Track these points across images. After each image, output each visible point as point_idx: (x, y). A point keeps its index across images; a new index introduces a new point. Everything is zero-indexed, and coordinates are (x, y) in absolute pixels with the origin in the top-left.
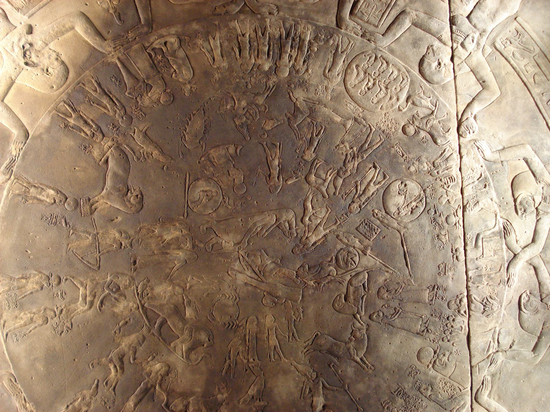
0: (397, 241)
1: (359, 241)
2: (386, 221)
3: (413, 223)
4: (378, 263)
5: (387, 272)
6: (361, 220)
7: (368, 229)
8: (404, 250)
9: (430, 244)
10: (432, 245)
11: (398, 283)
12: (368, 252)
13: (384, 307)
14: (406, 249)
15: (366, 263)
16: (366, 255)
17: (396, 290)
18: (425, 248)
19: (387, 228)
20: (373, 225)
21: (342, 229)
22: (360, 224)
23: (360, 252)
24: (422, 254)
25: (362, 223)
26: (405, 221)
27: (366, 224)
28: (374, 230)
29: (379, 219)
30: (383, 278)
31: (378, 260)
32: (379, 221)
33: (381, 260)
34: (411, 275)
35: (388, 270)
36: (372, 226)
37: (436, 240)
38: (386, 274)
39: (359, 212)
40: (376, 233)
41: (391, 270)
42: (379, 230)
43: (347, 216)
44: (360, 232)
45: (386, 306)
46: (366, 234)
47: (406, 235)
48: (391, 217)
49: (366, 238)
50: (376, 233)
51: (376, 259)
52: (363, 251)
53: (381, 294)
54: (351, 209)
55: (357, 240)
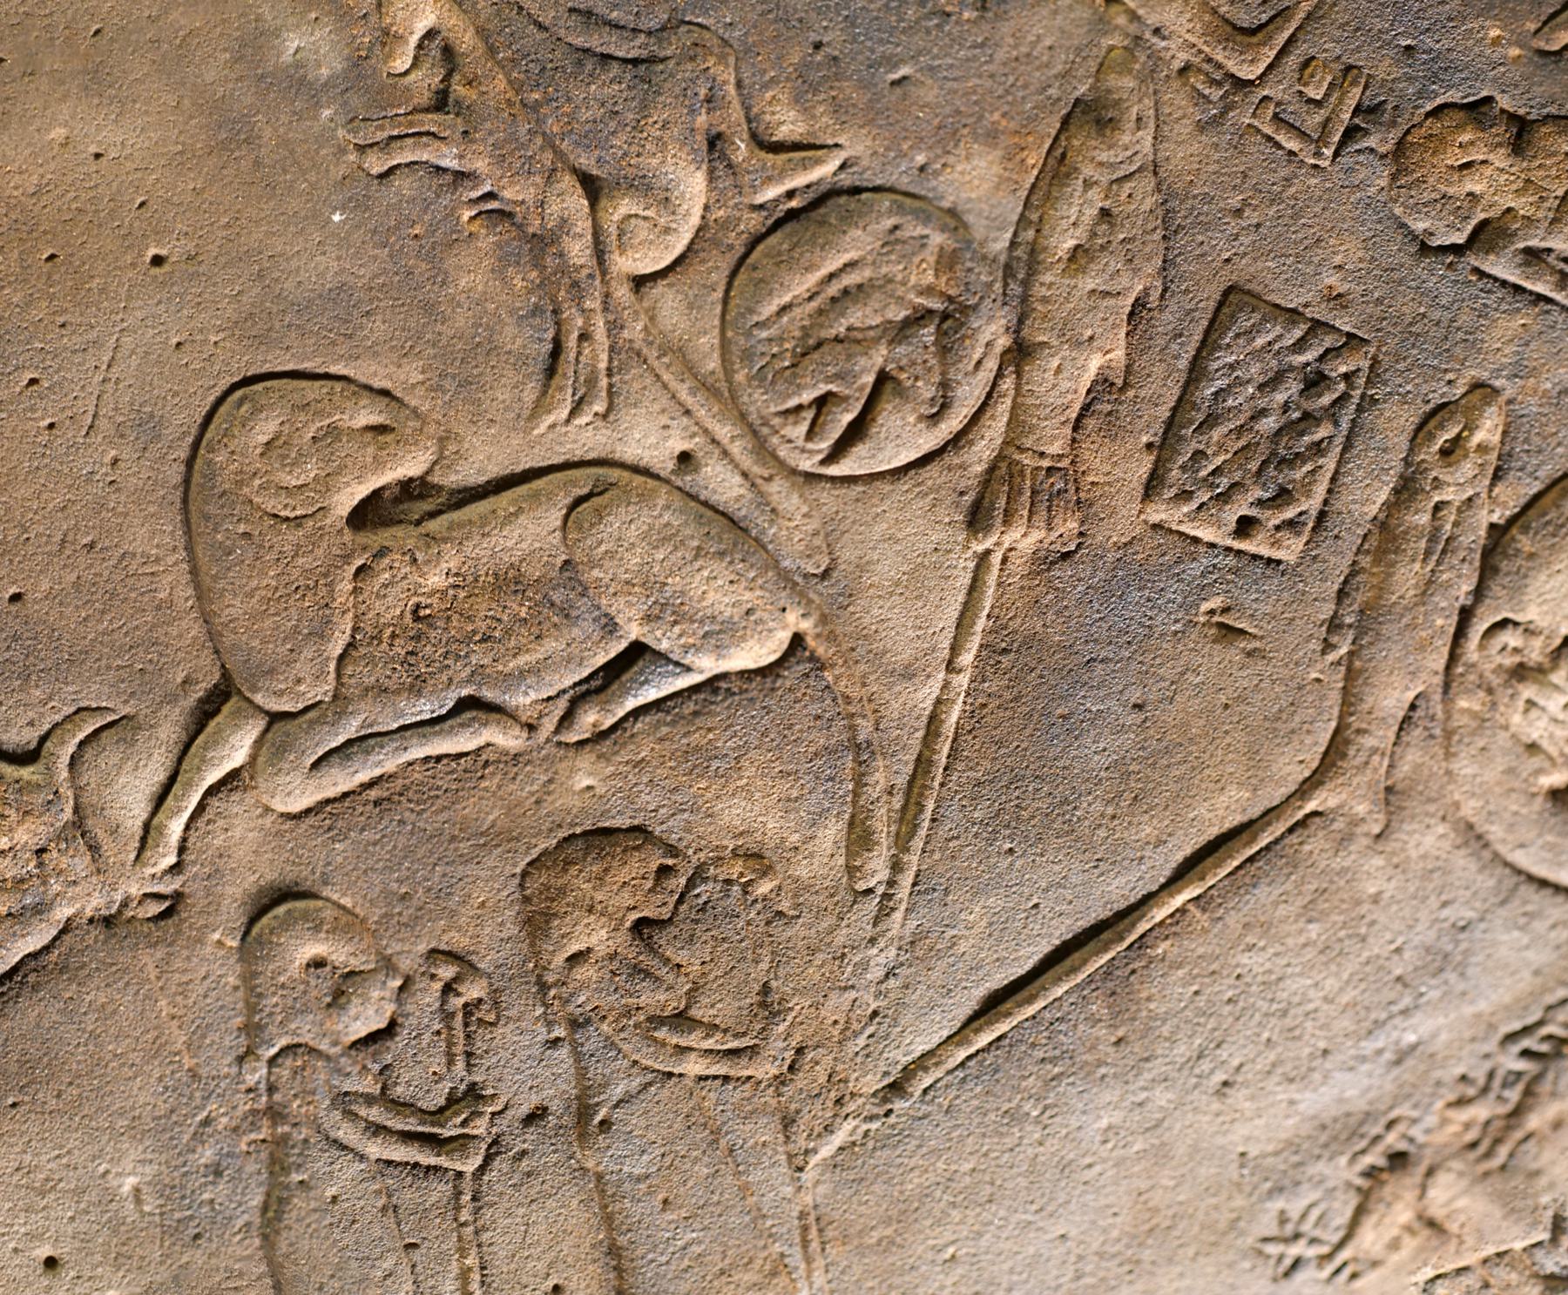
0: (1220, 785)
1: (1103, 384)
2: (1408, 576)
3: (1464, 864)
4: (926, 695)
5: (859, 838)
6: (1337, 300)
7: (1269, 424)
8: (1148, 900)
9: (1289, 1126)
10: (1291, 1145)
11: (768, 1005)
12: (1013, 535)
13: (447, 972)
14: (1160, 914)
15: (887, 568)
16: (977, 519)
17: (681, 1020)
18: (1238, 1097)
19: (1334, 625)
20: (1329, 463)
21: (1185, 129)
22: (1294, 315)
23: (982, 451)
24: (1162, 1097)
25: (1317, 326)
26: (1464, 766)
27: (1315, 382)
28: (1283, 496)
29: (1407, 489)
30: (772, 826)
31: (962, 681)
32: (1392, 507)
33: (973, 714)
34: (896, 1088)
35: (882, 826)
36: (1318, 449)
37: (1343, 1171)
38: (832, 832)
39: (1425, 249)
40: (1245, 526)
41: (896, 867)
42: (1290, 550)
43: (1351, 133)
44: (1207, 345)
45: (473, 991)
46: (1211, 421)
47: (1315, 844)
48: (1466, 615)
49: (1163, 448)
50: (1245, 526)
51: (967, 658)
52: (1002, 471)
53: (580, 882)
54: (1438, 143)
55: (1119, 354)
